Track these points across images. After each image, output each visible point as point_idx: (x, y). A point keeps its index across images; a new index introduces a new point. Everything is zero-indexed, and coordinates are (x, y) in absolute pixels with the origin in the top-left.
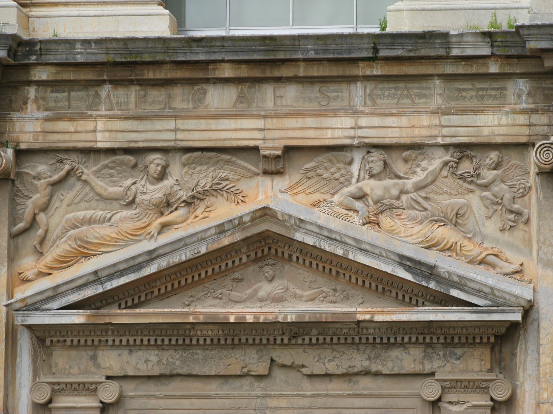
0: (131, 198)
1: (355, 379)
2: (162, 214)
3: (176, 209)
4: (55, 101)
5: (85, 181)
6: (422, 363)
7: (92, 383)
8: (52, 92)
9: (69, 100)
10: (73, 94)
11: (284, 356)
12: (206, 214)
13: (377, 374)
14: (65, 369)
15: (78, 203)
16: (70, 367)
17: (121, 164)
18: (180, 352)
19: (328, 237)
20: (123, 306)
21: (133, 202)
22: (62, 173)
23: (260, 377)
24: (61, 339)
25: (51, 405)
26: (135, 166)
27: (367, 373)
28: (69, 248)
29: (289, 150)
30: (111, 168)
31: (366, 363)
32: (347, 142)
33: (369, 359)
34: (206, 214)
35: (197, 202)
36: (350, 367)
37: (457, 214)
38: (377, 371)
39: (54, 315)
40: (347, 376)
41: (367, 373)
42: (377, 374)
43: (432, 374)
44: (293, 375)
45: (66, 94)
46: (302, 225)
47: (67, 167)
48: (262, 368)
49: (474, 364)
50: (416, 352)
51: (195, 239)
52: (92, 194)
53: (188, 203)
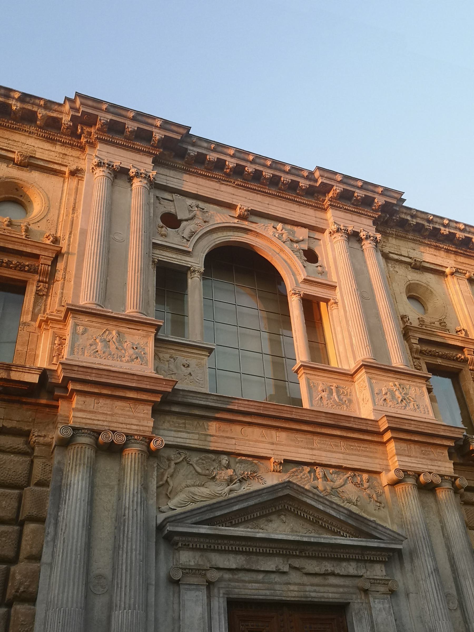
0: (214, 475)
1: (326, 577)
2: (228, 485)
3: (234, 484)
4: (179, 424)
5: (191, 464)
6: (357, 570)
7: (203, 570)
8: (177, 419)
9: (185, 424)
10: (187, 421)
11: (297, 563)
12: (248, 488)
13: (338, 575)
14: (187, 562)
15: (187, 475)
16: (189, 560)
17: (208, 458)
18: (245, 556)
19: (317, 500)
20: (224, 525)
21: (214, 478)
22: (181, 459)
23: (284, 573)
24: (187, 544)
25: (180, 582)
26: (214, 460)
27: (333, 574)
28: (185, 496)
29: (287, 462)
30: (203, 460)
31: (332, 569)
32: (310, 461)
33: (333, 566)
34: (248, 488)
35: (244, 481)
36: (325, 570)
37: (357, 501)
38: (338, 573)
39: (189, 527)
40: (326, 575)
41: (333, 574)
42: (338, 575)
43: (361, 576)
44: (298, 573)
45: (184, 421)
46: (306, 493)
47: (183, 457)
48: (286, 569)
49: (378, 571)
50: (353, 564)
51: (257, 494)
52: (194, 472)
53: (240, 481)
